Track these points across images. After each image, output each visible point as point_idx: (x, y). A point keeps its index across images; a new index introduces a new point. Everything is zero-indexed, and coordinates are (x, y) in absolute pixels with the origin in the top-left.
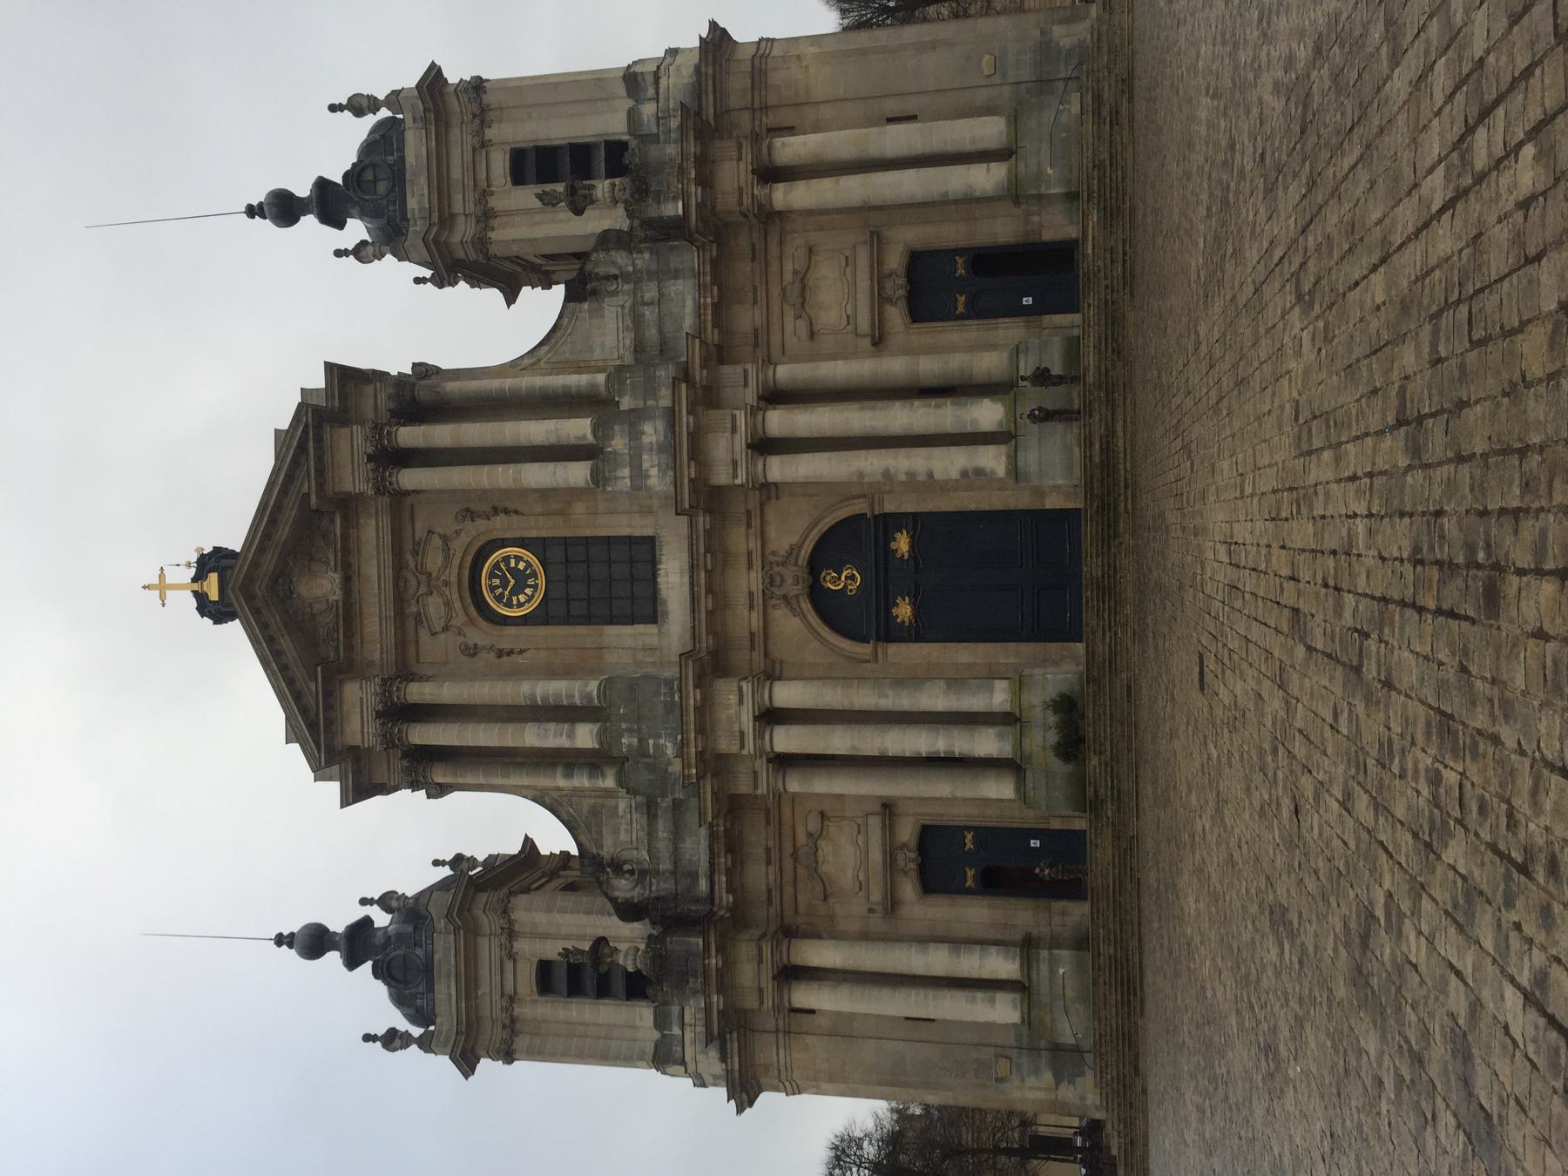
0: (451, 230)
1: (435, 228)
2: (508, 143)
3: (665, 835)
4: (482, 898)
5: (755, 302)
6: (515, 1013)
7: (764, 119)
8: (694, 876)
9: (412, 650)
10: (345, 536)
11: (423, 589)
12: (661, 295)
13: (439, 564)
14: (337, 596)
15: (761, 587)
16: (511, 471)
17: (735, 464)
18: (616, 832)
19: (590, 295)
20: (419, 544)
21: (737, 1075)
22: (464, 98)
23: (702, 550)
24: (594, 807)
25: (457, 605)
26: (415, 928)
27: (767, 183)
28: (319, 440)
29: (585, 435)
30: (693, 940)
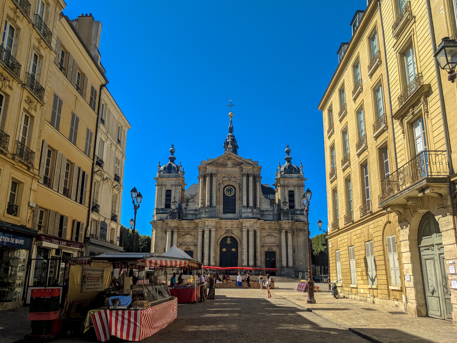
8: (186, 217)
12: (270, 215)
18: (192, 205)
28: (251, 166)
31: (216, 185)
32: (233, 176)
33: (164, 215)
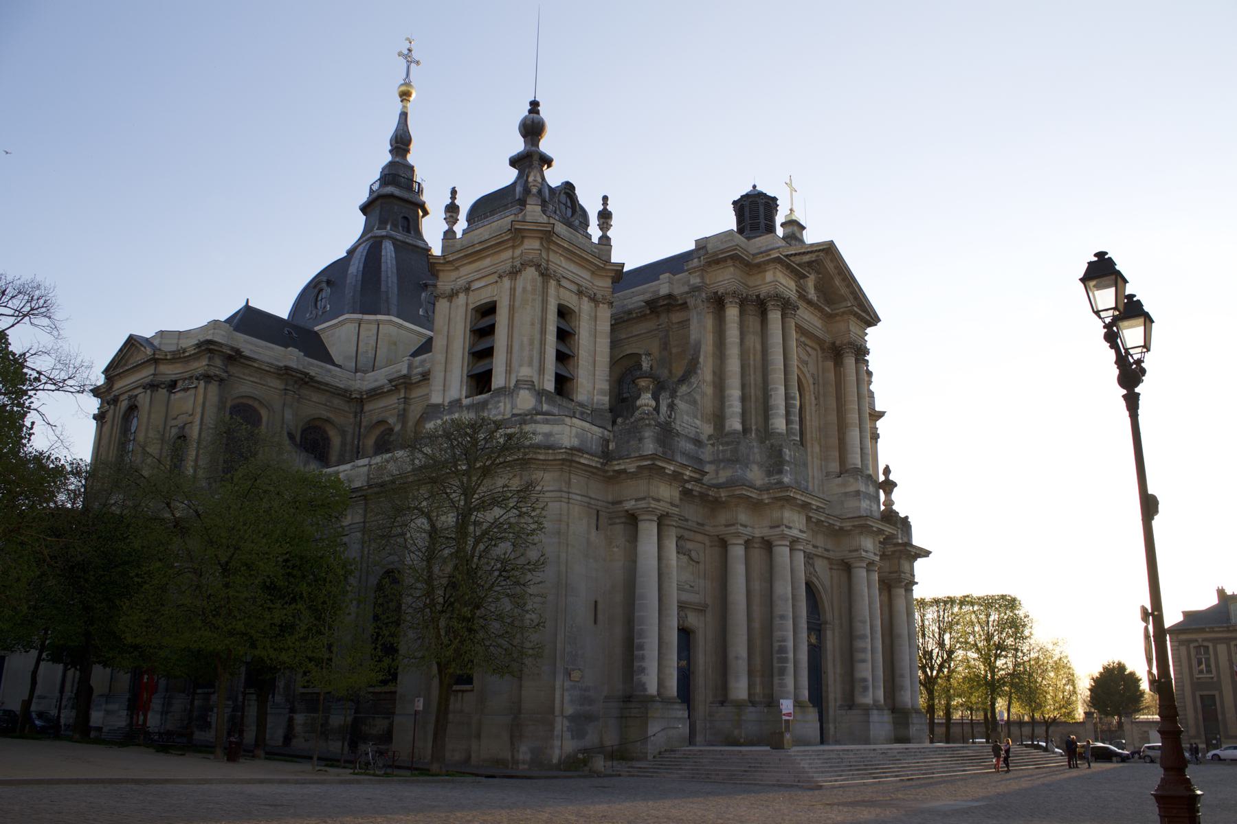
10: (821, 310)
21: (577, 459)
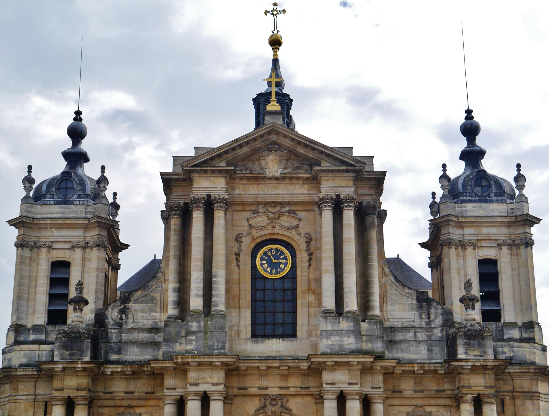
0: (456, 226)
1: (455, 219)
2: (500, 259)
3: (141, 337)
4: (104, 233)
5: (415, 391)
6: (42, 249)
7: (508, 398)
8: (119, 352)
9: (240, 208)
10: (298, 179)
11: (271, 215)
12: (420, 342)
13: (283, 224)
14: (269, 175)
15: (270, 394)
16: (330, 268)
17: (333, 384)
18: (143, 311)
19: (421, 305)
20: (294, 212)
21: (14, 373)
22: (523, 236)
23: (290, 364)
24: (156, 299)
25: (263, 233)
26: (88, 195)
27: (474, 401)
28: (347, 171)
29: (347, 307)
30: (89, 354)
31: (227, 241)
32: (287, 208)
33: (43, 347)
